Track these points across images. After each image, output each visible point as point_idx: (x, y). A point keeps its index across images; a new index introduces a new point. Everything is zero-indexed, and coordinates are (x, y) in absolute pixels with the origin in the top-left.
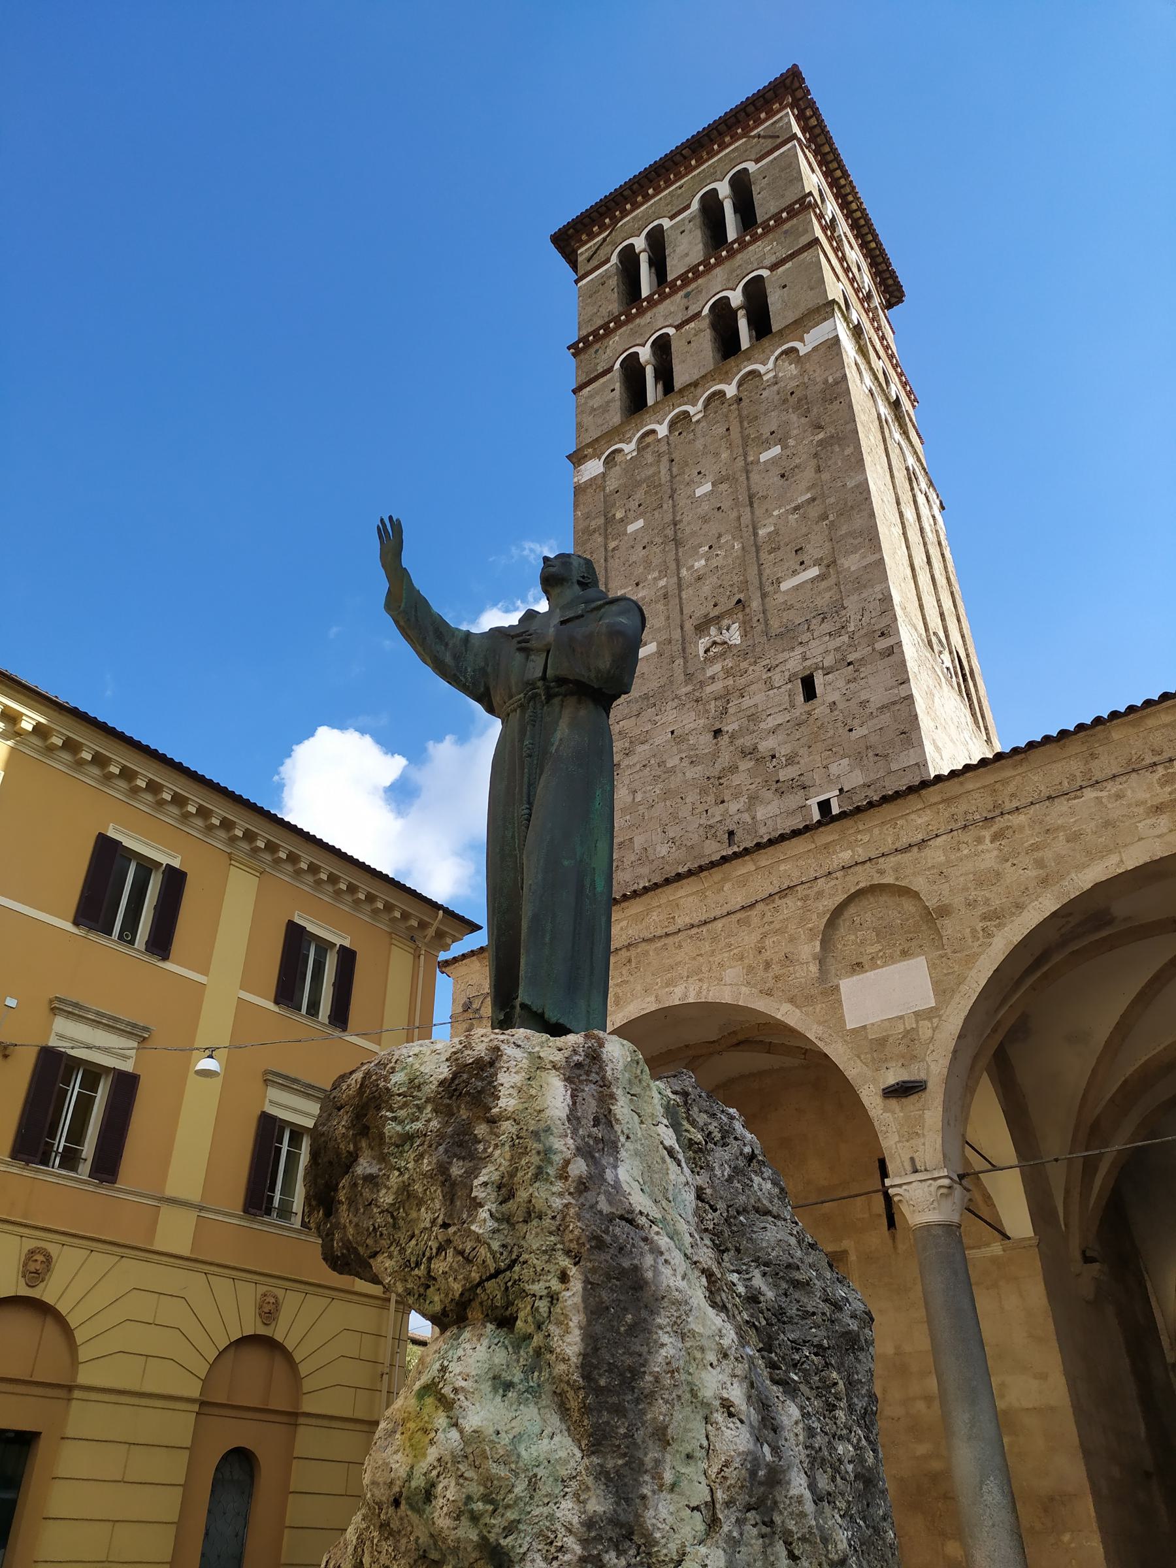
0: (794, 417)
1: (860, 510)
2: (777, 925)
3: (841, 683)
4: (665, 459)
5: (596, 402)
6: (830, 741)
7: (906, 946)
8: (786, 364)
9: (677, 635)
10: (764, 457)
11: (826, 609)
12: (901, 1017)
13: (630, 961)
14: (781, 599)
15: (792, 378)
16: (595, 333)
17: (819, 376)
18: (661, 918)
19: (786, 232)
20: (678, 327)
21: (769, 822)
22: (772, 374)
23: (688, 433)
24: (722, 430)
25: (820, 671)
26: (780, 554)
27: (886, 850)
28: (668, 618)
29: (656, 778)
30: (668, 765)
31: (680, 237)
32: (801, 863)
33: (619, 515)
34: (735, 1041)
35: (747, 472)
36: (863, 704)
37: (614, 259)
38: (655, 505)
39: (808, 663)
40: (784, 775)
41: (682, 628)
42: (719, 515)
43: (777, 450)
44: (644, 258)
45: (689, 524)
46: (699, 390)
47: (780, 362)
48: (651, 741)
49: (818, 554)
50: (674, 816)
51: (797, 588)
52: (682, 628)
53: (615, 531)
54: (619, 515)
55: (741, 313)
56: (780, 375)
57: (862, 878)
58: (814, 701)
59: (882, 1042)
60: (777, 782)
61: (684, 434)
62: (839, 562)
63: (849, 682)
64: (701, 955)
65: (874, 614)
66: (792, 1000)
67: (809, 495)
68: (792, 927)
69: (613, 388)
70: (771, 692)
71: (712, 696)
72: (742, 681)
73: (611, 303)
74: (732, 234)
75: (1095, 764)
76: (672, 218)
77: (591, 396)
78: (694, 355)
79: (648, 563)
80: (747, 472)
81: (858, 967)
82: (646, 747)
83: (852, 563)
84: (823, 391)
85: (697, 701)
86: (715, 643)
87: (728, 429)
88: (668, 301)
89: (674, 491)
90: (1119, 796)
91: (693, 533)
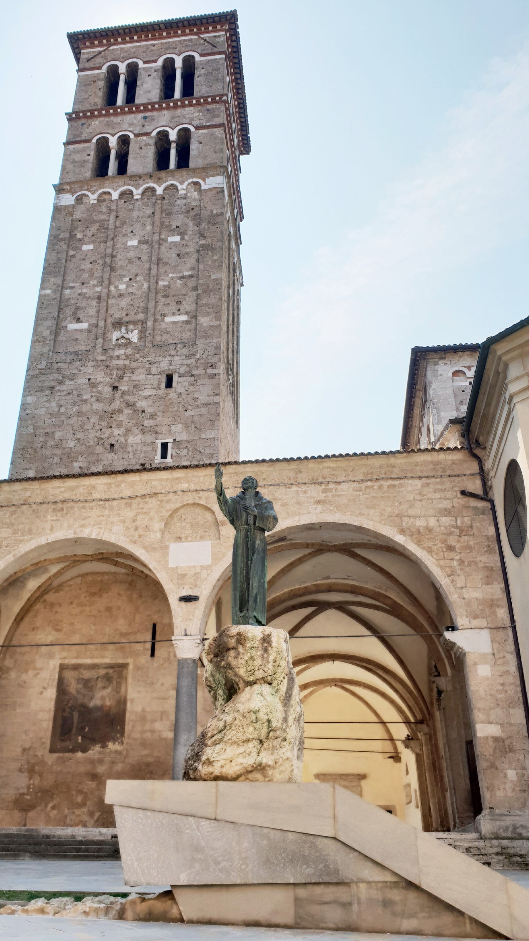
0: (191, 224)
1: (215, 294)
2: (145, 510)
3: (186, 384)
4: (113, 214)
5: (77, 157)
6: (174, 413)
7: (203, 534)
8: (193, 190)
9: (101, 323)
10: (171, 239)
11: (186, 341)
12: (194, 567)
13: (62, 509)
14: (164, 326)
15: (195, 200)
16: (85, 112)
17: (209, 207)
18: (85, 491)
19: (208, 110)
20: (137, 135)
21: (134, 446)
22: (184, 192)
24: (149, 212)
25: (177, 374)
26: (168, 300)
27: (204, 488)
28: (98, 311)
29: (75, 403)
30: (85, 397)
31: (148, 78)
32: (163, 483)
33: (79, 236)
34: (100, 557)
35: (160, 244)
36: (195, 399)
37: (104, 69)
38: (102, 239)
39: (171, 367)
40: (147, 423)
41: (105, 321)
42: (139, 262)
43: (177, 239)
44: (122, 78)
45: (120, 260)
46: (141, 182)
47: (189, 187)
48: (76, 380)
49: (188, 308)
50: (82, 428)
51: (174, 323)
52: (105, 321)
53: (74, 245)
54: (79, 236)
55: (173, 145)
56: (189, 195)
57: (190, 498)
58: (171, 389)
59: (184, 576)
61: (128, 203)
62: (198, 318)
63: (190, 385)
64: (103, 516)
65: (210, 354)
66: (145, 548)
67: (190, 273)
68: (152, 513)
69: (89, 154)
70: (149, 376)
71: (116, 367)
72: (134, 365)
73: (98, 98)
74: (178, 93)
75: (300, 476)
76: (145, 62)
77: (74, 152)
78: (142, 159)
79: (91, 273)
80: (160, 244)
81: (179, 539)
82: (72, 383)
83: (205, 321)
84: (210, 216)
85: (107, 367)
86: (123, 337)
87: (153, 213)
88: (132, 116)
89: (115, 236)
90: (305, 492)
91: (122, 267)
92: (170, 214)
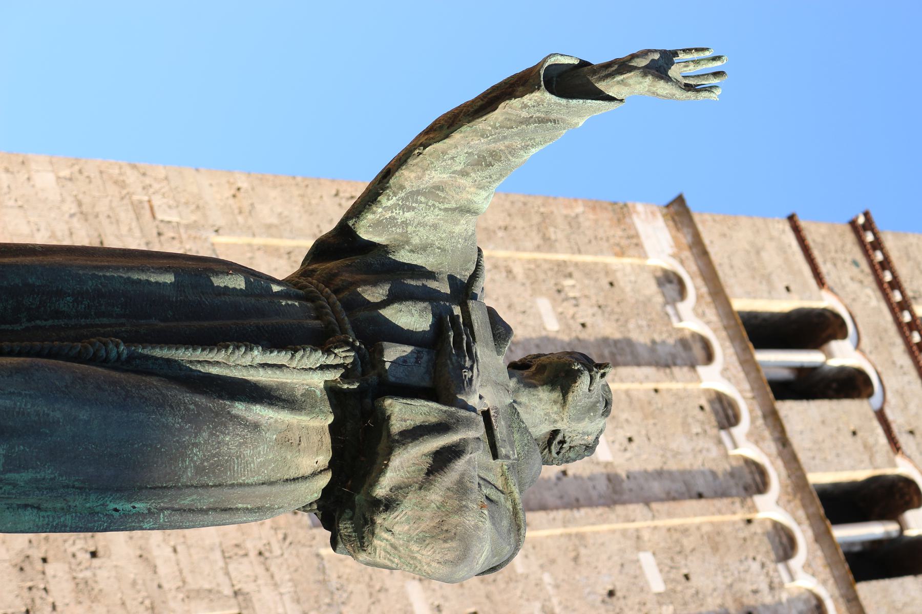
10: (647, 560)
23: (703, 423)
43: (657, 585)
46: (772, 446)
60: (44, 560)
61: (700, 415)
70: (217, 555)
92: (715, 549)
